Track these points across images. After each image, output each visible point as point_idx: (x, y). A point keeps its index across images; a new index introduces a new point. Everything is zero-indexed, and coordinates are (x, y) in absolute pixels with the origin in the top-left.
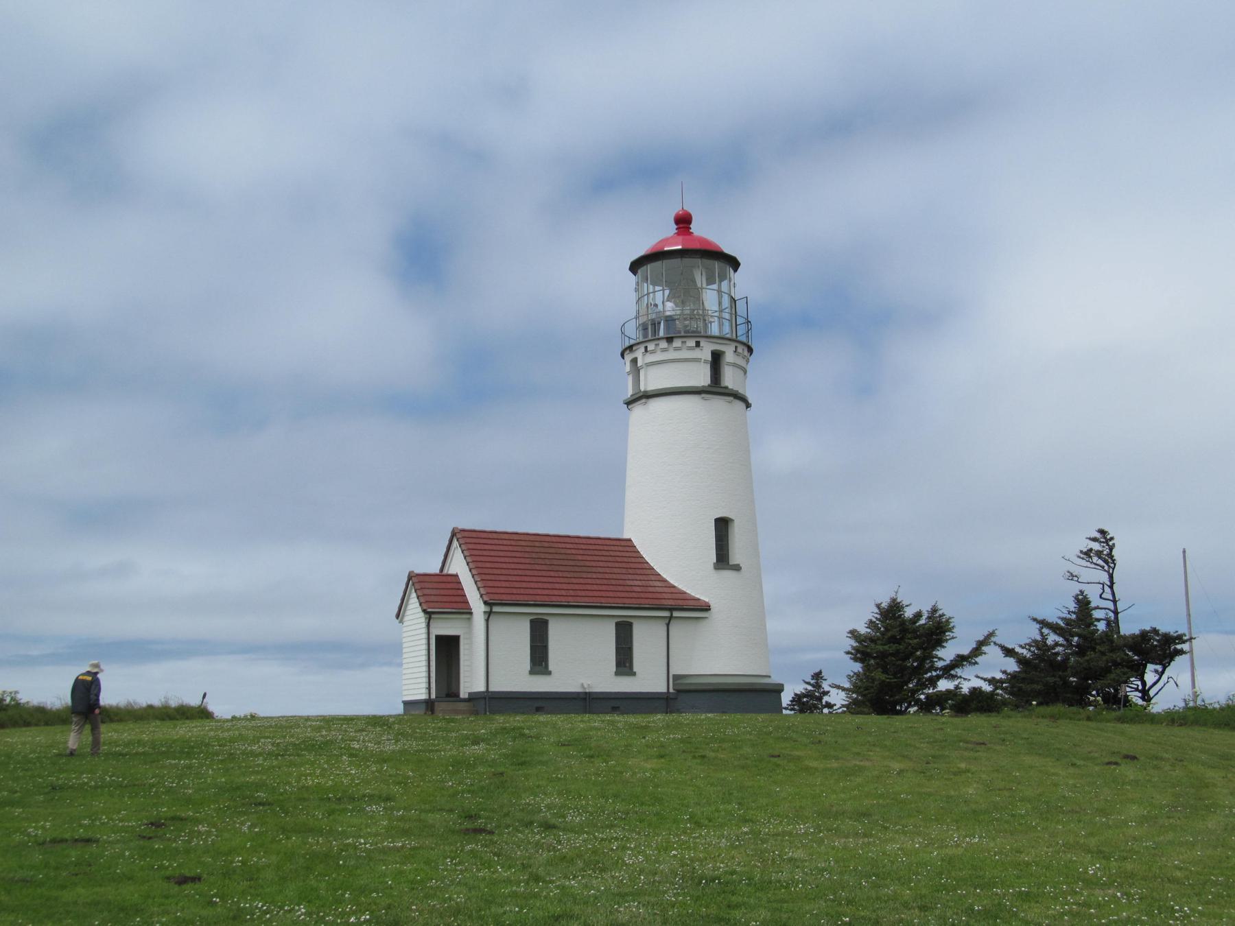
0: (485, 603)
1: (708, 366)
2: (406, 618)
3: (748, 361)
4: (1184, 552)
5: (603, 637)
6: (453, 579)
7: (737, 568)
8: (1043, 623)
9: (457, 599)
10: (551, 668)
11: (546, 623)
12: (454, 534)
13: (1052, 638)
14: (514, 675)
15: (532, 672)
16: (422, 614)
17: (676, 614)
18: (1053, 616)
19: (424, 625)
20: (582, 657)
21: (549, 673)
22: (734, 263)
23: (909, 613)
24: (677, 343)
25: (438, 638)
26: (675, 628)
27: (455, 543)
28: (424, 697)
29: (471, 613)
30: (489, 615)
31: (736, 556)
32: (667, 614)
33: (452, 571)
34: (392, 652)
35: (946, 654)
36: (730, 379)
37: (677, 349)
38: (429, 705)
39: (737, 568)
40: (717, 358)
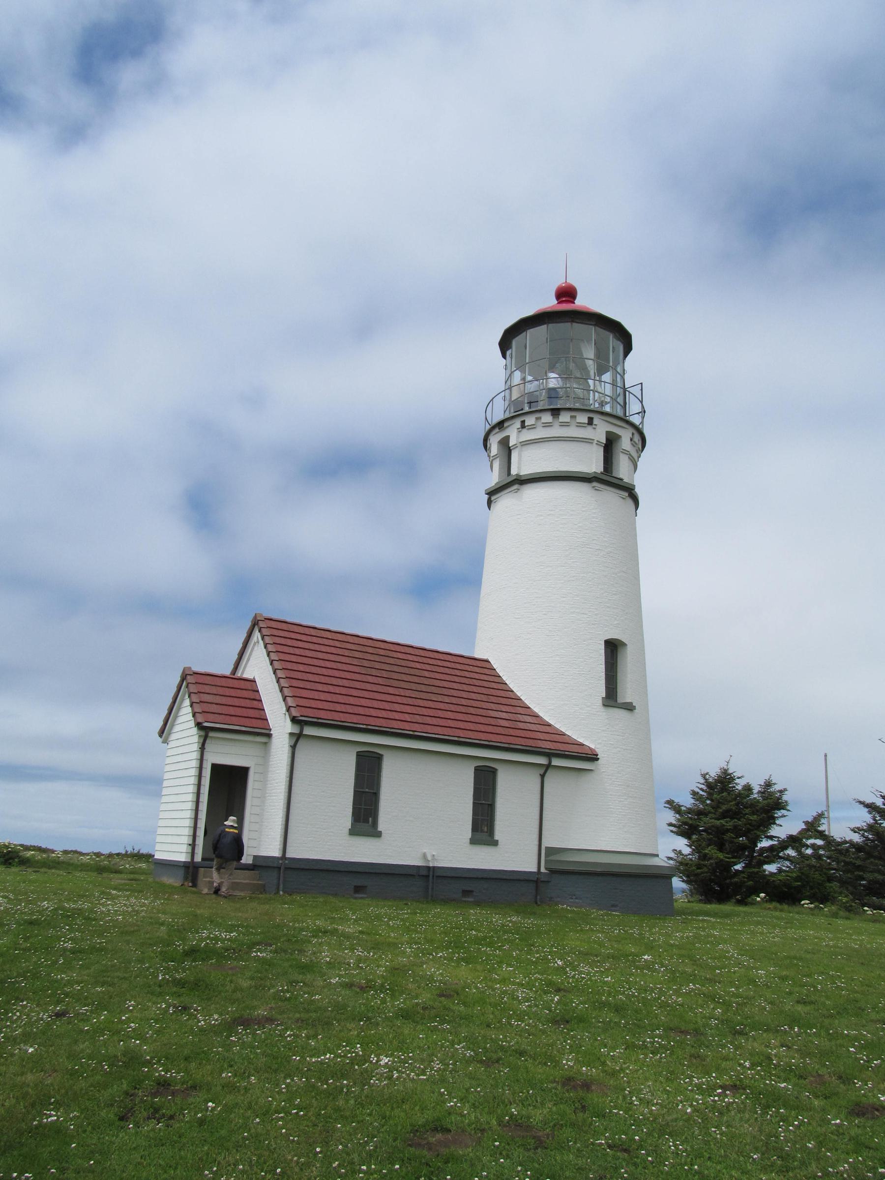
0: (294, 720)
1: (601, 450)
2: (173, 737)
4: (826, 756)
5: (460, 784)
6: (248, 685)
7: (629, 707)
9: (251, 713)
10: (381, 827)
11: (379, 758)
12: (255, 623)
15: (353, 832)
16: (195, 730)
17: (556, 762)
19: (196, 747)
21: (378, 835)
23: (740, 784)
24: (565, 417)
25: (215, 767)
27: (257, 635)
28: (183, 858)
29: (269, 736)
30: (297, 738)
31: (626, 694)
32: (543, 760)
33: (247, 675)
34: (149, 784)
36: (622, 469)
39: (629, 707)
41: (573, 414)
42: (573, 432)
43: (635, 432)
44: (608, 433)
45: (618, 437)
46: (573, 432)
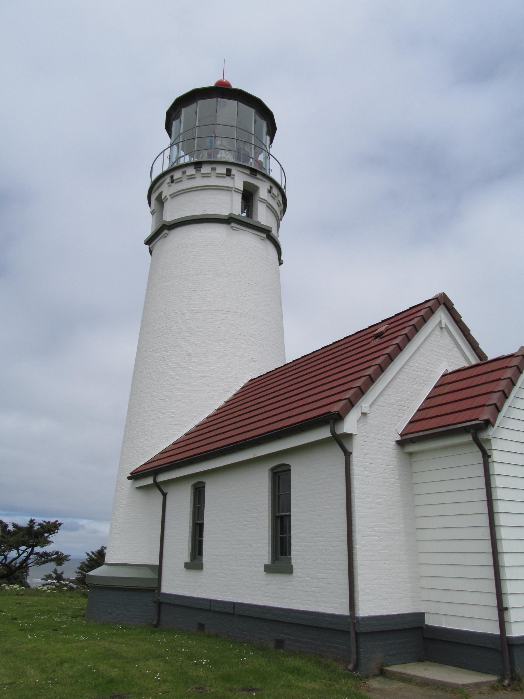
1: (241, 195)
3: (278, 221)
24: (206, 169)
36: (263, 216)
37: (206, 176)
41: (214, 166)
42: (213, 181)
43: (272, 185)
44: (246, 184)
45: (257, 188)
46: (213, 181)
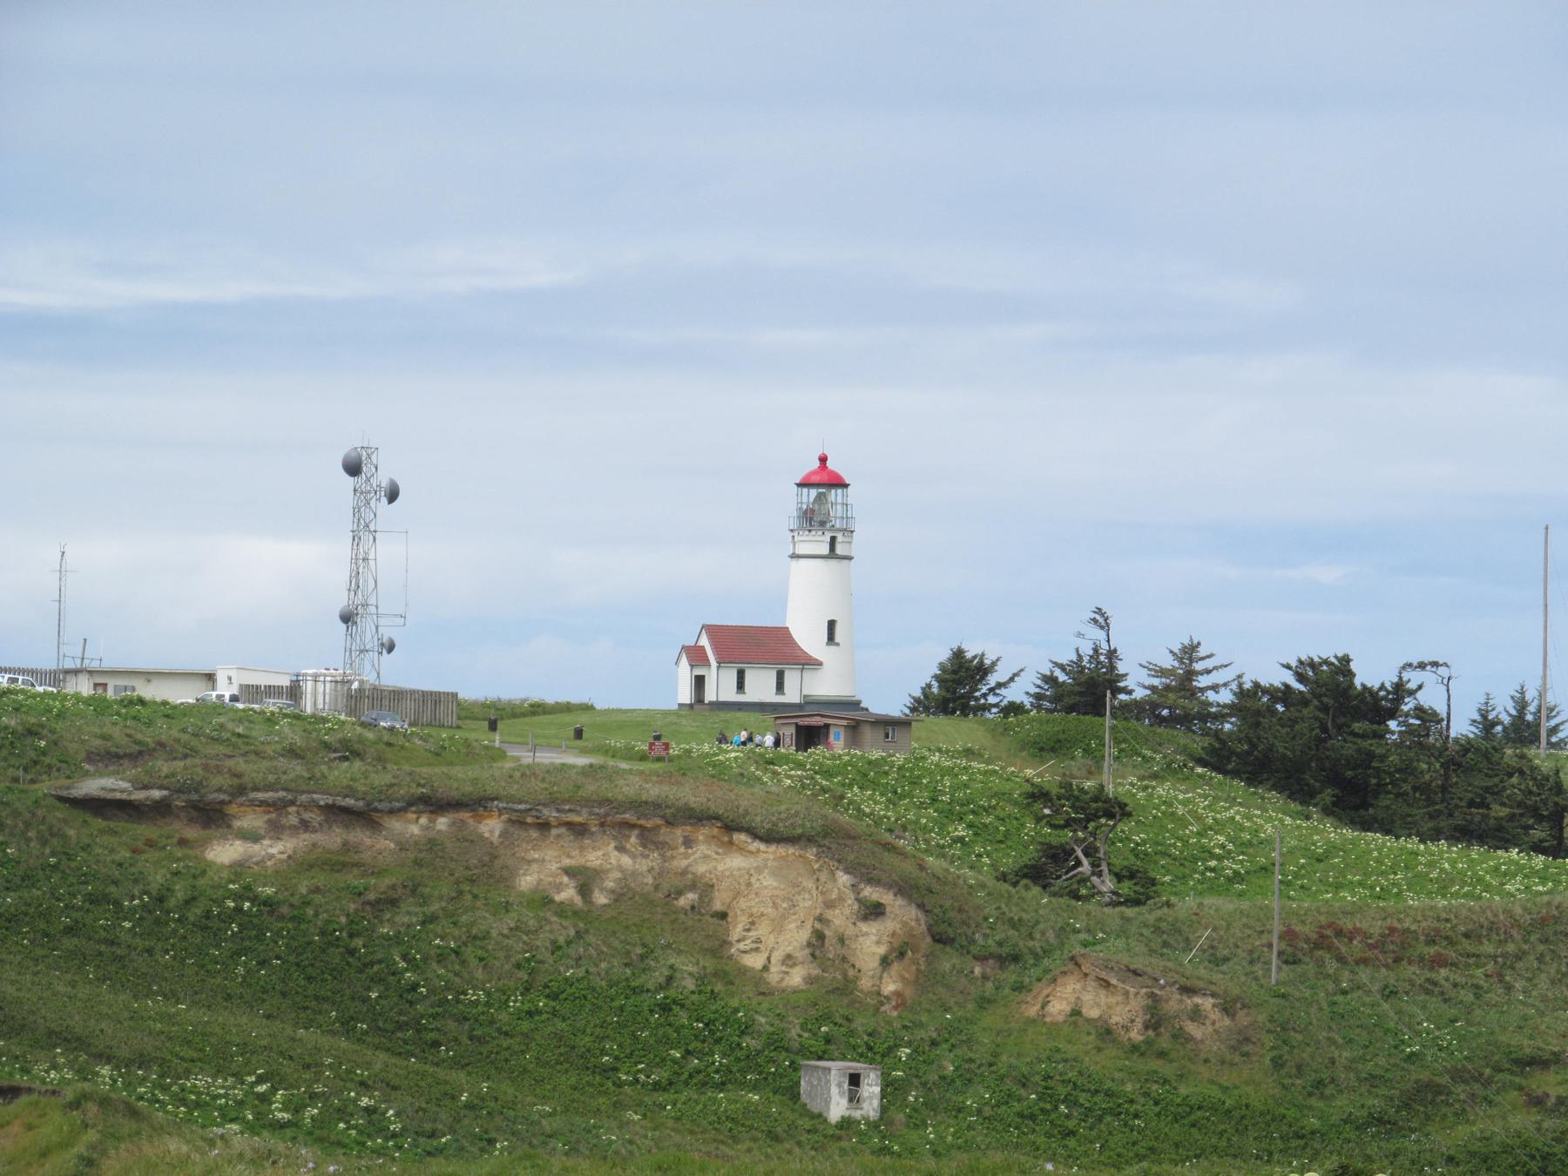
5: (772, 677)
8: (1056, 664)
13: (1058, 673)
14: (729, 694)
18: (1063, 660)
20: (761, 686)
22: (846, 486)
23: (969, 655)
26: (806, 674)
31: (838, 639)
35: (992, 680)
36: (839, 550)
38: (691, 706)
40: (833, 539)
